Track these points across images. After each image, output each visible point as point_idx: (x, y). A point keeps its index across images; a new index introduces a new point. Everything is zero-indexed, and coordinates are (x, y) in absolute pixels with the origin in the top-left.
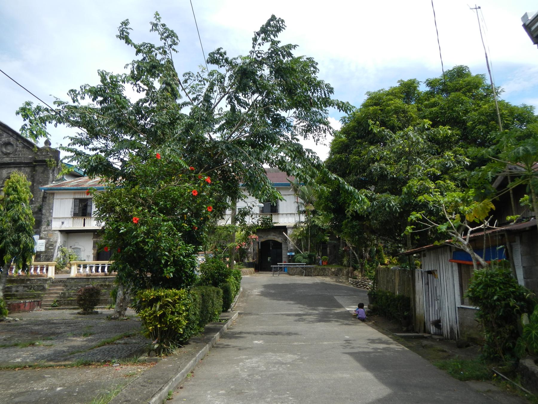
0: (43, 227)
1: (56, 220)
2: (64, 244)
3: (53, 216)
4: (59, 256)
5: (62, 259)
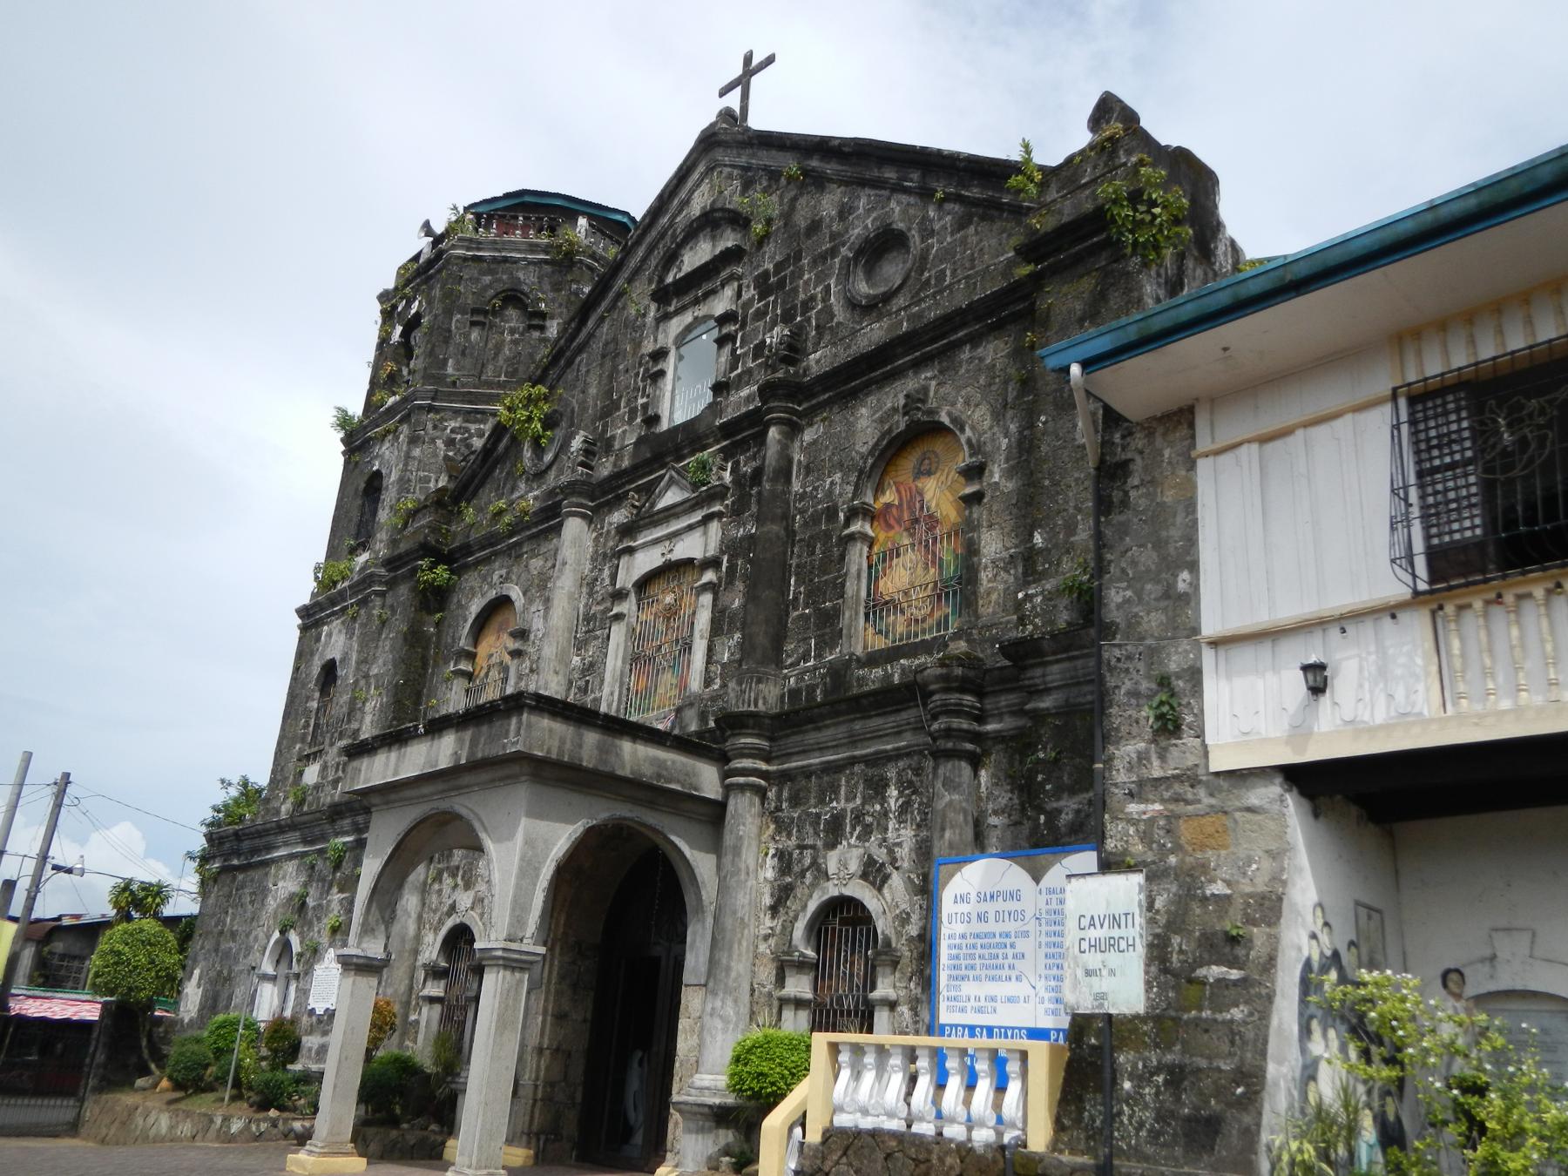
0: (1128, 753)
1: (1244, 655)
2: (1372, 935)
3: (1210, 626)
4: (1327, 1088)
5: (1368, 1133)
